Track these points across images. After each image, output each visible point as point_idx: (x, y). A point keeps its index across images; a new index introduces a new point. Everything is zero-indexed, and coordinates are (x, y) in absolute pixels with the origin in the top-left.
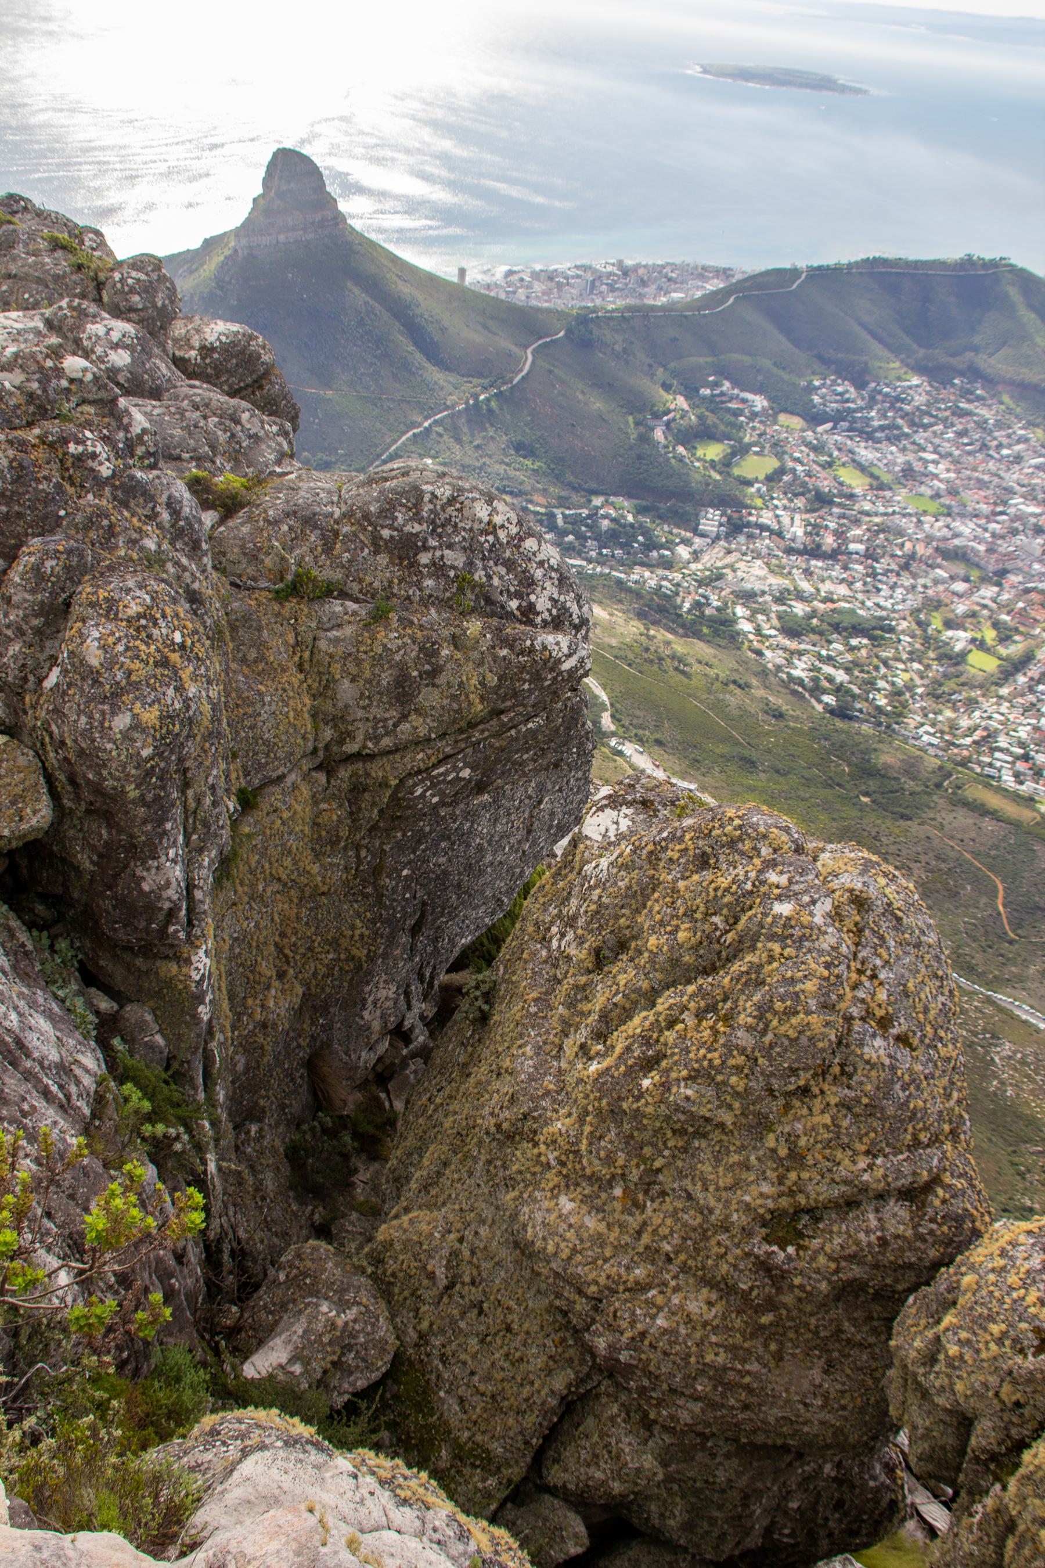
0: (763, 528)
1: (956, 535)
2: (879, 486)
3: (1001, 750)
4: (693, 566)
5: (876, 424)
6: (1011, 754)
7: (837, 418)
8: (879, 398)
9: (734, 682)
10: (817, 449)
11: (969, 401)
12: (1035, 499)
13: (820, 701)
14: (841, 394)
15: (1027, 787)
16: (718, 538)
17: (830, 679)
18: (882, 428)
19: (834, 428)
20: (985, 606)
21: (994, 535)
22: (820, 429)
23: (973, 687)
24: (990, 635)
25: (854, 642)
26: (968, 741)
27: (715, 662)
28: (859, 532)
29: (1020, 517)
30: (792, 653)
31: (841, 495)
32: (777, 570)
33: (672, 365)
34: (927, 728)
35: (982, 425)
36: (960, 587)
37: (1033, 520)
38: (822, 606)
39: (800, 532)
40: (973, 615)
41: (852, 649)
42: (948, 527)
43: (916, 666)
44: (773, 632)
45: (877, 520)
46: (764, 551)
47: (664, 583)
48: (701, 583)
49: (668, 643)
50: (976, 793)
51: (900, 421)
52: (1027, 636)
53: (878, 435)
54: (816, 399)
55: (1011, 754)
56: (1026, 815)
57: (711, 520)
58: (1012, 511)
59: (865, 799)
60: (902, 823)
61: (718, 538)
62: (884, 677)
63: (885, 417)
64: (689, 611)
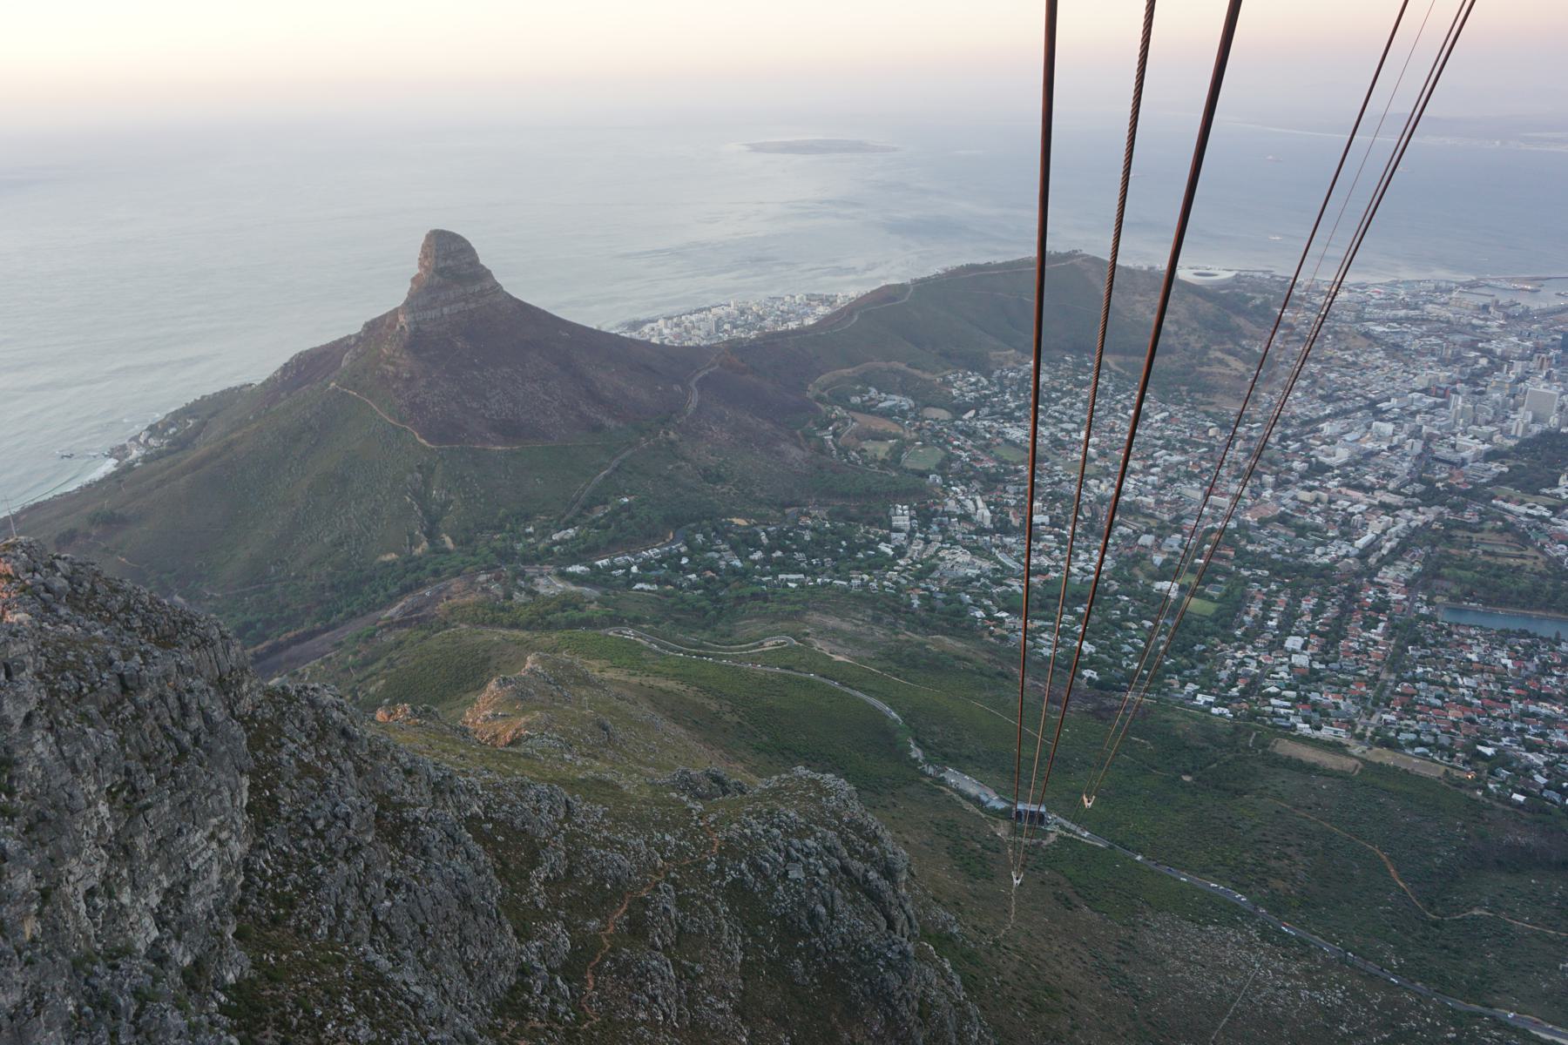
0: (950, 515)
3: (1277, 696)
4: (901, 562)
5: (1013, 405)
7: (977, 404)
8: (1007, 382)
9: (1000, 674)
10: (970, 433)
12: (1174, 449)
14: (974, 384)
15: (1326, 733)
16: (913, 531)
18: (1019, 408)
19: (977, 414)
20: (1175, 553)
21: (1154, 487)
22: (966, 417)
24: (1191, 579)
25: (1080, 610)
26: (1234, 691)
27: (970, 655)
32: (975, 550)
34: (1190, 687)
36: (1147, 540)
37: (1183, 468)
39: (987, 513)
40: (1167, 562)
41: (1079, 617)
43: (1148, 624)
44: (1004, 614)
46: (959, 537)
48: (920, 576)
49: (921, 645)
50: (1285, 748)
54: (955, 392)
55: (1287, 700)
56: (1348, 764)
57: (902, 517)
58: (1160, 462)
59: (1187, 778)
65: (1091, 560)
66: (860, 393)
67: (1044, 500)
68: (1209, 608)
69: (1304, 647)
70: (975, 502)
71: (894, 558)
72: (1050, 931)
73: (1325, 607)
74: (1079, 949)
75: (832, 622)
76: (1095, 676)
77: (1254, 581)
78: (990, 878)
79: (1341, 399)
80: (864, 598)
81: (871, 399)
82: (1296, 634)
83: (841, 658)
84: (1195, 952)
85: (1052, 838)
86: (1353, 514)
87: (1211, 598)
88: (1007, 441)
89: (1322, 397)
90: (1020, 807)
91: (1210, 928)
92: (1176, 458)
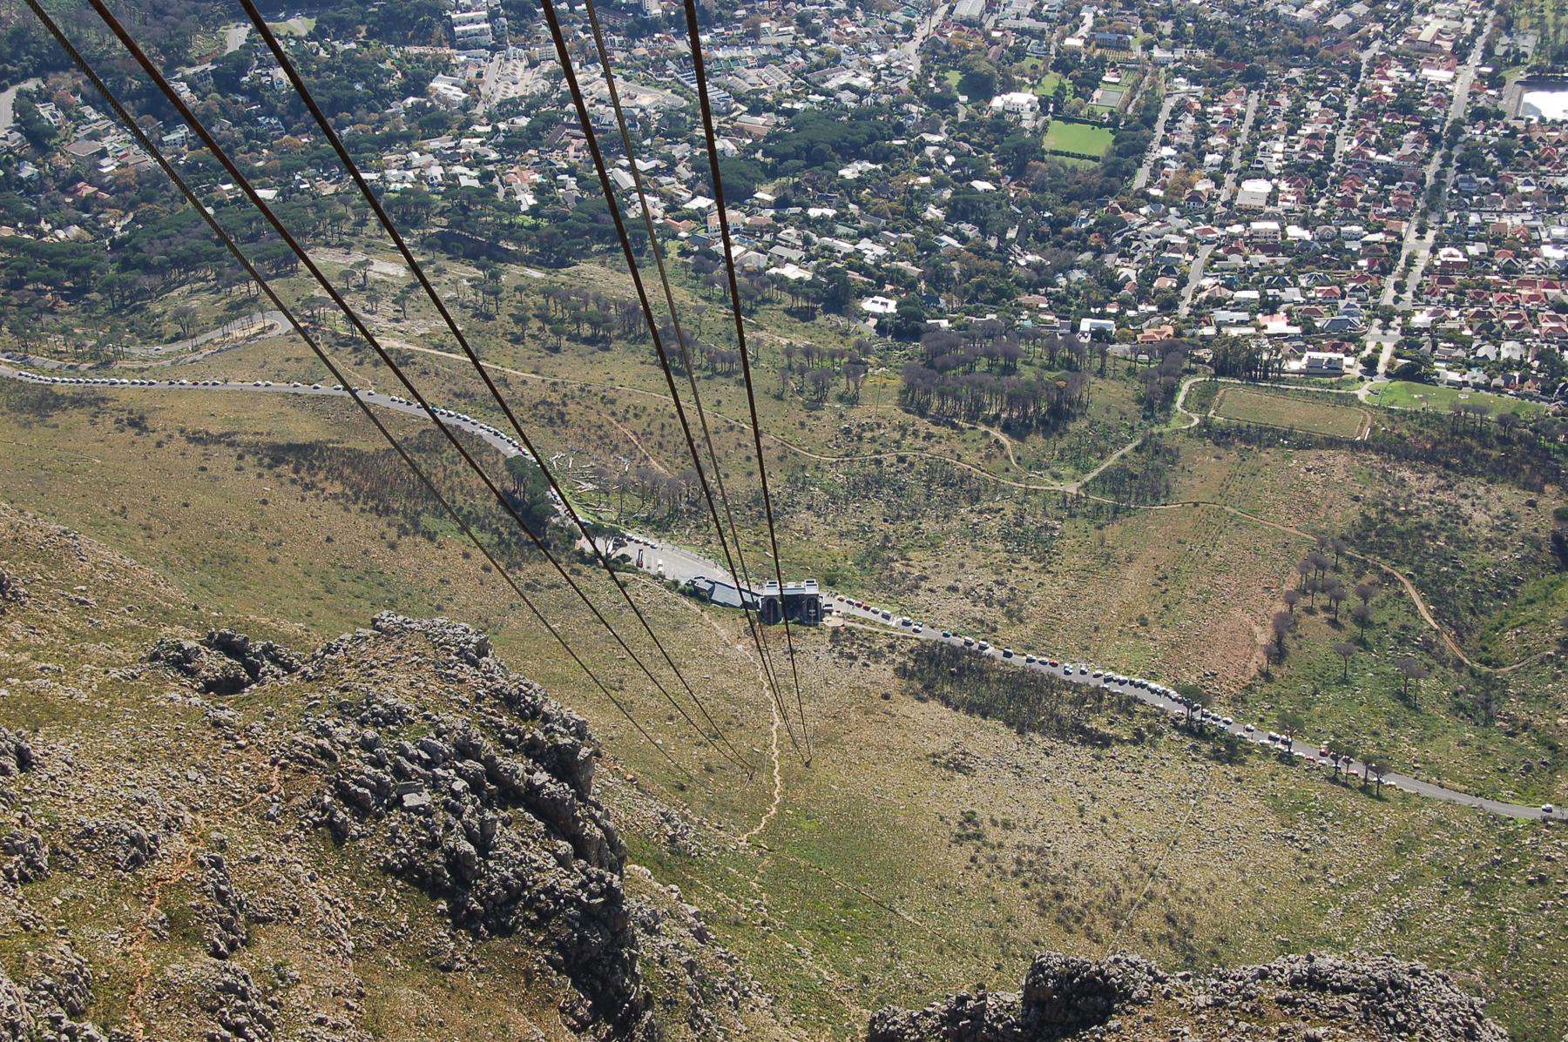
6: (1239, 306)
17: (855, 261)
55: (1239, 306)
69: (1272, 198)
71: (465, 107)
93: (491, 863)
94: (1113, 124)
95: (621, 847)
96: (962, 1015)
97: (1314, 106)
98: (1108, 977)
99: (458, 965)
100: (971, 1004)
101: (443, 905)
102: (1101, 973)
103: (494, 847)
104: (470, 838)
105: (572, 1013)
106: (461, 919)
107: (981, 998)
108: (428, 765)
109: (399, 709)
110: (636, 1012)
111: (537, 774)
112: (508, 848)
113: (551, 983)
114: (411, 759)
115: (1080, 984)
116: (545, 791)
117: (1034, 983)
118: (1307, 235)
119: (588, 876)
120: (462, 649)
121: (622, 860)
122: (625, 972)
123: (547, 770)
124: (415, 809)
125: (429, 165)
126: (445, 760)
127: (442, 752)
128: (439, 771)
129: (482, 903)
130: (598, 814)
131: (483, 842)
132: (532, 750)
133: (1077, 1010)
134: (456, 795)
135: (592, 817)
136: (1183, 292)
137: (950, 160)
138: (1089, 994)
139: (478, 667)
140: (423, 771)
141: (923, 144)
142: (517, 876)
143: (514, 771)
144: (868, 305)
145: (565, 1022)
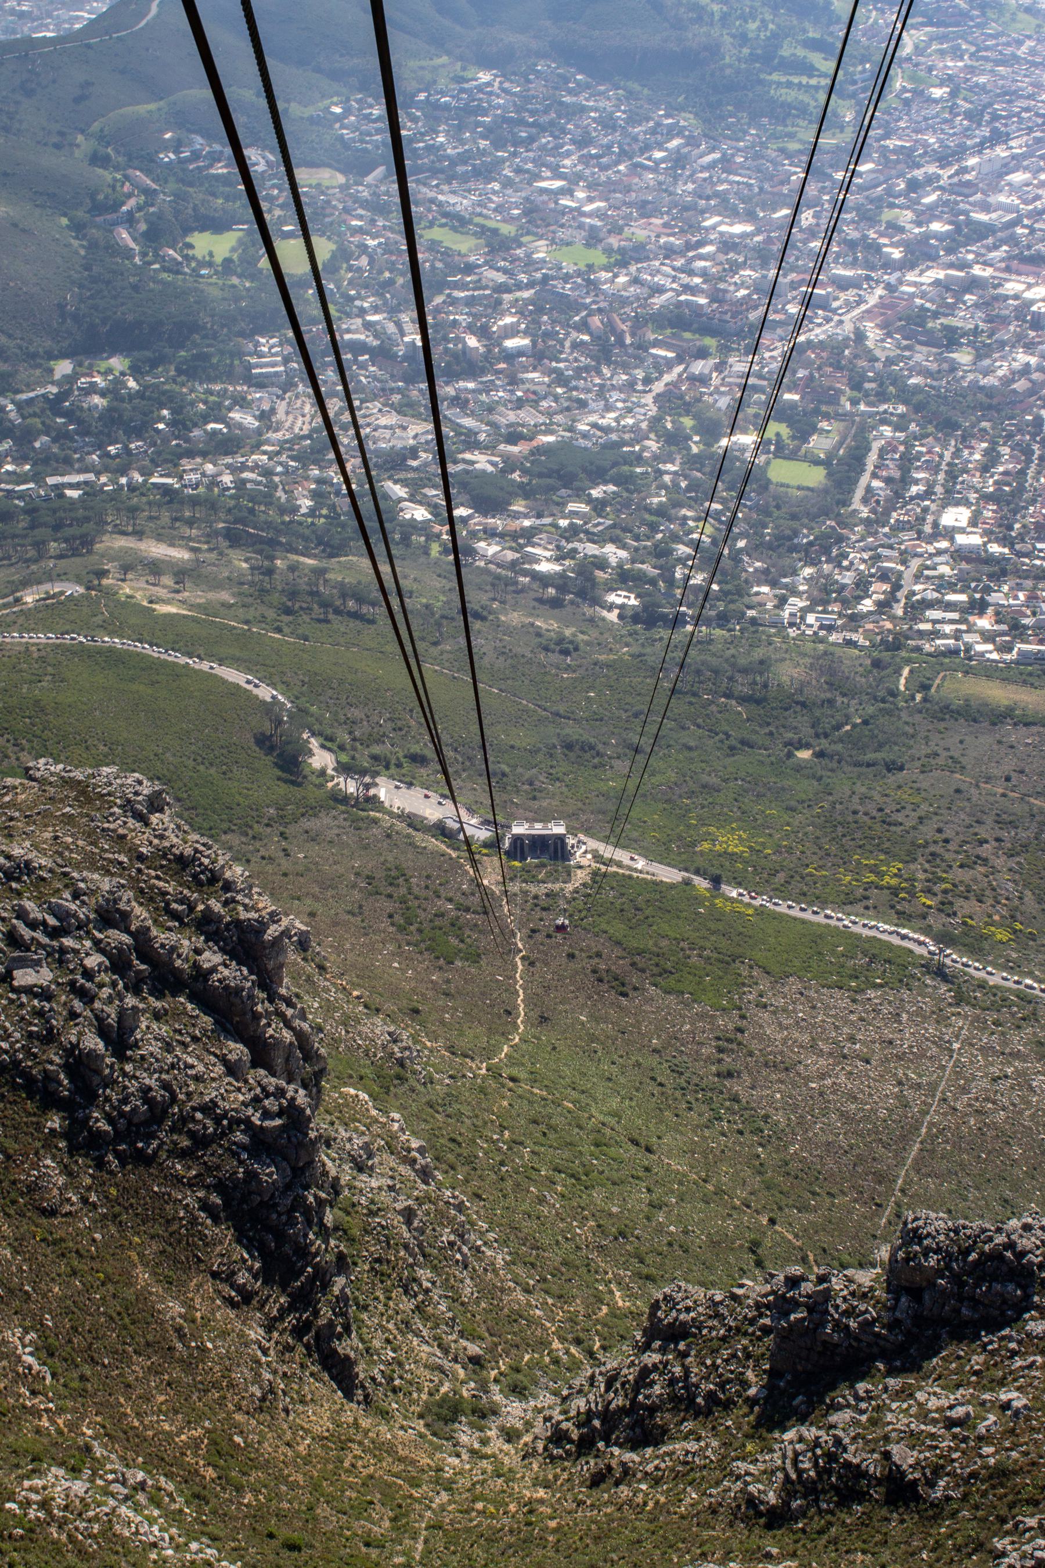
1: (660, 290)
2: (497, 245)
6: (949, 606)
11: (570, 92)
13: (610, 607)
17: (601, 563)
18: (463, 158)
22: (369, 179)
23: (813, 518)
25: (596, 493)
26: (867, 605)
28: (508, 320)
29: (728, 244)
30: (514, 536)
31: (454, 269)
33: (96, 126)
35: (608, 124)
36: (699, 367)
38: (515, 449)
41: (599, 507)
42: (636, 281)
45: (526, 294)
47: (246, 475)
51: (483, 143)
52: (839, 417)
53: (460, 169)
55: (949, 606)
59: (804, 754)
60: (892, 779)
61: (288, 386)
62: (675, 538)
63: (462, 142)
64: (312, 512)
65: (608, 408)
66: (177, 146)
67: (520, 313)
68: (815, 477)
69: (973, 522)
70: (398, 324)
71: (259, 432)
72: (593, 1038)
73: (999, 455)
74: (653, 1061)
75: (158, 550)
76: (633, 602)
77: (884, 422)
78: (474, 957)
79: (995, 117)
80: (208, 503)
81: (196, 156)
82: (957, 503)
83: (173, 610)
84: (852, 1039)
85: (581, 877)
86: (1033, 302)
87: (817, 462)
88: (446, 215)
89: (969, 115)
90: (518, 829)
91: (871, 993)
92: (738, 229)
93: (129, 1068)
94: (826, 463)
95: (319, 1057)
96: (795, 1304)
97: (1005, 450)
98: (1023, 1254)
99: (68, 1208)
100: (807, 1287)
101: (55, 1122)
102: (1011, 1245)
103: (136, 1046)
104: (103, 1031)
105: (229, 1278)
106: (81, 1141)
107: (822, 1279)
108: (54, 933)
109: (28, 863)
110: (322, 1279)
111: (207, 954)
112: (155, 1047)
113: (203, 1237)
114: (33, 925)
115: (976, 1263)
116: (216, 977)
117: (907, 1260)
118: (1006, 551)
119: (264, 1089)
120: (129, 801)
121: (320, 1074)
122: (309, 1223)
123: (223, 950)
124: (28, 990)
125: (220, 474)
126: (79, 928)
127: (75, 915)
128: (68, 942)
129: (110, 1120)
130: (290, 1012)
131: (119, 1039)
132: (207, 926)
133: (975, 1302)
134: (88, 974)
135: (281, 1015)
136: (899, 595)
137: (683, 485)
138: (994, 1278)
139: (147, 824)
140: (45, 940)
141: (660, 473)
142: (166, 1086)
143: (173, 949)
144: (612, 598)
145: (218, 1292)
